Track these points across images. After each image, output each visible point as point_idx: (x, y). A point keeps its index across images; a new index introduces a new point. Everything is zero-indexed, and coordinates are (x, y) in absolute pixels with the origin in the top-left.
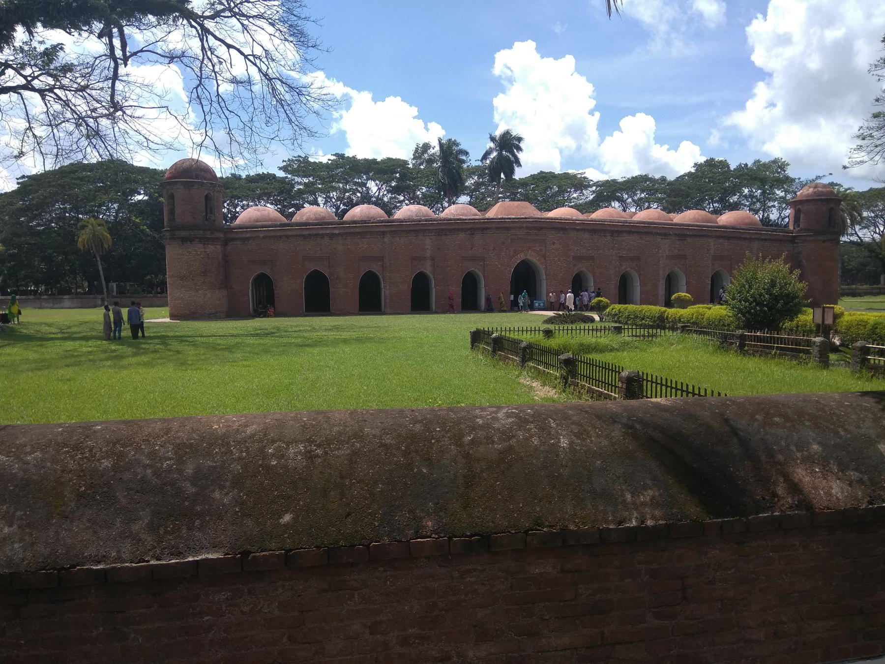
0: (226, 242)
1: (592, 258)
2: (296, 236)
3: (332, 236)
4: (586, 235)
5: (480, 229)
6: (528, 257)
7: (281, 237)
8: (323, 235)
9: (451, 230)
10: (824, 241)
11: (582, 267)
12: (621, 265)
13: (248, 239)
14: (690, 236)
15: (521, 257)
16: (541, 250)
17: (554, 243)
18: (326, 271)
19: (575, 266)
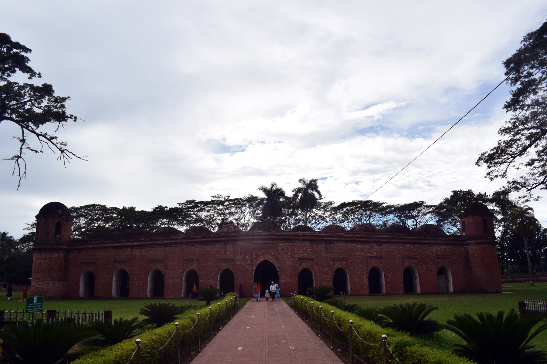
1: (312, 259)
2: (110, 247)
3: (132, 247)
4: (308, 244)
6: (266, 259)
7: (101, 248)
8: (127, 247)
10: (482, 244)
11: (305, 265)
12: (335, 264)
13: (82, 249)
14: (385, 242)
15: (261, 259)
16: (275, 254)
17: (283, 249)
19: (300, 265)
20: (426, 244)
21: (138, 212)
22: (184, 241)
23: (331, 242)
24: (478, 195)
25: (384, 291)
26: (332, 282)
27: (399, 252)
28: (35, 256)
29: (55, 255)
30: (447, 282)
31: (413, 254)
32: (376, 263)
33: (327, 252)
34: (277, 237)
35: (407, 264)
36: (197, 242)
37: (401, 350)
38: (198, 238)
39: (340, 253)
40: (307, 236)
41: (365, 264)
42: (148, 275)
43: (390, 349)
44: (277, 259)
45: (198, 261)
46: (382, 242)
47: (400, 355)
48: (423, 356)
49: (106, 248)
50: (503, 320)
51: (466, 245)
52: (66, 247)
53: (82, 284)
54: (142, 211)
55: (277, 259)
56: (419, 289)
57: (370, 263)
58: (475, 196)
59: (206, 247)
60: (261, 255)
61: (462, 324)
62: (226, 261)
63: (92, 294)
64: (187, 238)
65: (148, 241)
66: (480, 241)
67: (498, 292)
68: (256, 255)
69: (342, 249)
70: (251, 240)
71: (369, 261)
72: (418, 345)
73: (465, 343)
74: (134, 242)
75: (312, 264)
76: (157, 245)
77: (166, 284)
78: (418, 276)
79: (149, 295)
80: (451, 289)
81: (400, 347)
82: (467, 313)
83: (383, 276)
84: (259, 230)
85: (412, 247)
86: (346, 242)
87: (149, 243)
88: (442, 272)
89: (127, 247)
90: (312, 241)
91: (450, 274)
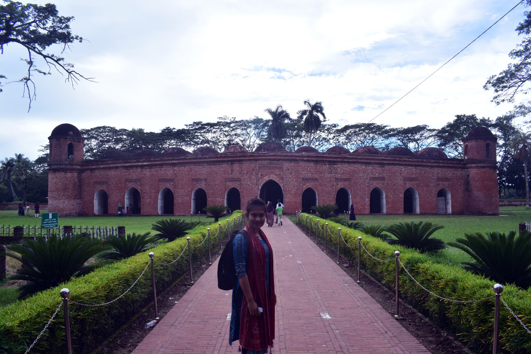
0: (81, 172)
1: (316, 179)
2: (121, 167)
3: (142, 167)
4: (312, 164)
5: (237, 160)
7: (112, 168)
8: (137, 166)
9: (217, 162)
10: (483, 167)
11: (309, 185)
12: (338, 184)
13: (94, 169)
15: (267, 178)
16: (280, 174)
17: (288, 169)
18: (139, 189)
19: (304, 184)
20: (428, 166)
21: (147, 133)
22: (192, 161)
23: (334, 163)
24: (481, 120)
25: (385, 211)
26: (335, 201)
27: (401, 174)
28: (50, 176)
29: (69, 175)
30: (446, 203)
31: (414, 176)
32: (378, 184)
33: (331, 173)
34: (281, 158)
35: (408, 185)
36: (204, 162)
37: (413, 266)
38: (205, 158)
39: (343, 174)
40: (311, 157)
41: (367, 185)
42: (158, 193)
43: (402, 264)
44: (282, 179)
45: (206, 180)
46: (384, 164)
47: (411, 271)
48: (437, 272)
49: (117, 168)
50: (515, 240)
51: (467, 168)
52: (78, 167)
53: (96, 203)
54: (151, 133)
55: (282, 179)
56: (418, 210)
57: (372, 184)
58: (479, 121)
59: (213, 166)
60: (267, 175)
61: (473, 243)
62: (233, 180)
63: (105, 212)
64: (195, 158)
65: (157, 161)
66: (481, 165)
67: (496, 214)
68: (262, 175)
69: (346, 170)
70: (257, 160)
71: (371, 181)
72: (430, 262)
73: (474, 261)
74: (144, 161)
75: (315, 184)
76: (167, 164)
77: (175, 202)
78: (418, 197)
79: (160, 212)
80: (450, 211)
81: (412, 264)
82: (480, 231)
83: (384, 196)
84: (264, 151)
85: (413, 169)
86: (349, 162)
87: (159, 163)
88: (442, 194)
89: (137, 166)
90: (316, 162)
91: (449, 196)
